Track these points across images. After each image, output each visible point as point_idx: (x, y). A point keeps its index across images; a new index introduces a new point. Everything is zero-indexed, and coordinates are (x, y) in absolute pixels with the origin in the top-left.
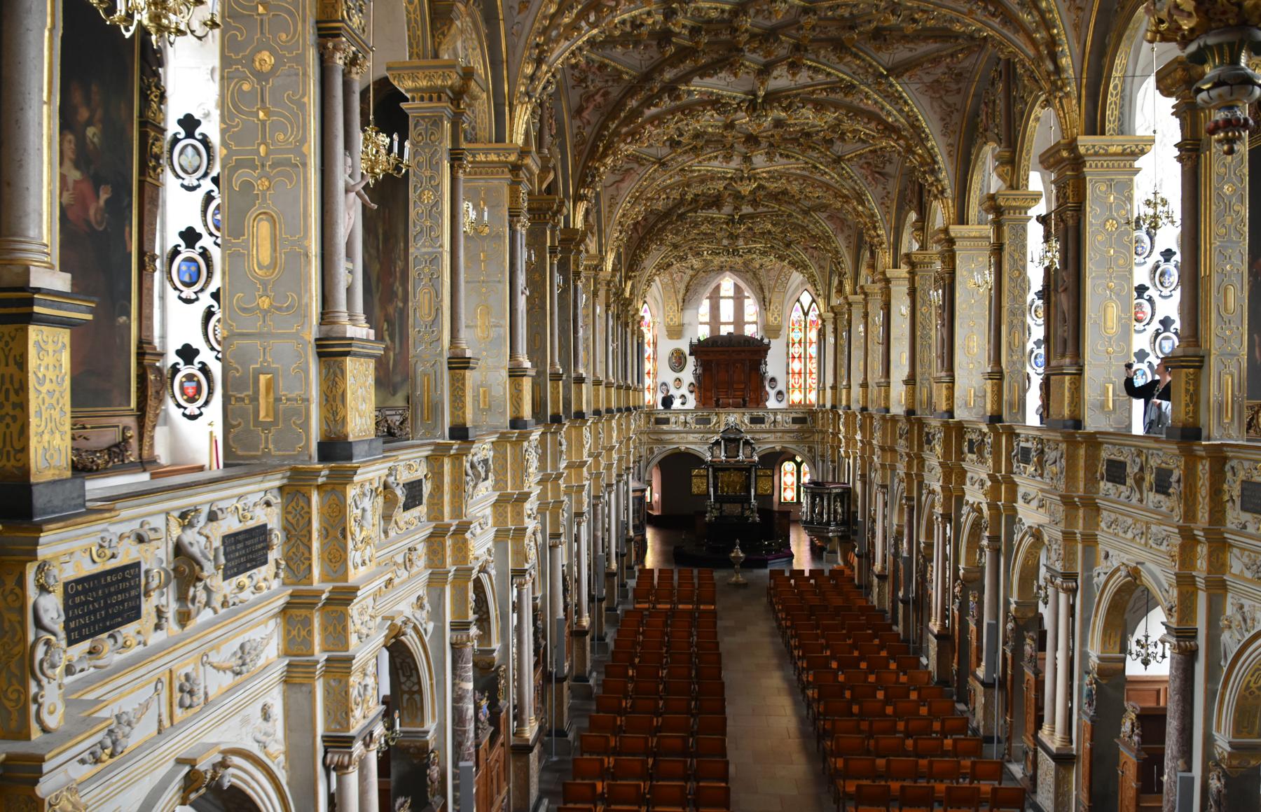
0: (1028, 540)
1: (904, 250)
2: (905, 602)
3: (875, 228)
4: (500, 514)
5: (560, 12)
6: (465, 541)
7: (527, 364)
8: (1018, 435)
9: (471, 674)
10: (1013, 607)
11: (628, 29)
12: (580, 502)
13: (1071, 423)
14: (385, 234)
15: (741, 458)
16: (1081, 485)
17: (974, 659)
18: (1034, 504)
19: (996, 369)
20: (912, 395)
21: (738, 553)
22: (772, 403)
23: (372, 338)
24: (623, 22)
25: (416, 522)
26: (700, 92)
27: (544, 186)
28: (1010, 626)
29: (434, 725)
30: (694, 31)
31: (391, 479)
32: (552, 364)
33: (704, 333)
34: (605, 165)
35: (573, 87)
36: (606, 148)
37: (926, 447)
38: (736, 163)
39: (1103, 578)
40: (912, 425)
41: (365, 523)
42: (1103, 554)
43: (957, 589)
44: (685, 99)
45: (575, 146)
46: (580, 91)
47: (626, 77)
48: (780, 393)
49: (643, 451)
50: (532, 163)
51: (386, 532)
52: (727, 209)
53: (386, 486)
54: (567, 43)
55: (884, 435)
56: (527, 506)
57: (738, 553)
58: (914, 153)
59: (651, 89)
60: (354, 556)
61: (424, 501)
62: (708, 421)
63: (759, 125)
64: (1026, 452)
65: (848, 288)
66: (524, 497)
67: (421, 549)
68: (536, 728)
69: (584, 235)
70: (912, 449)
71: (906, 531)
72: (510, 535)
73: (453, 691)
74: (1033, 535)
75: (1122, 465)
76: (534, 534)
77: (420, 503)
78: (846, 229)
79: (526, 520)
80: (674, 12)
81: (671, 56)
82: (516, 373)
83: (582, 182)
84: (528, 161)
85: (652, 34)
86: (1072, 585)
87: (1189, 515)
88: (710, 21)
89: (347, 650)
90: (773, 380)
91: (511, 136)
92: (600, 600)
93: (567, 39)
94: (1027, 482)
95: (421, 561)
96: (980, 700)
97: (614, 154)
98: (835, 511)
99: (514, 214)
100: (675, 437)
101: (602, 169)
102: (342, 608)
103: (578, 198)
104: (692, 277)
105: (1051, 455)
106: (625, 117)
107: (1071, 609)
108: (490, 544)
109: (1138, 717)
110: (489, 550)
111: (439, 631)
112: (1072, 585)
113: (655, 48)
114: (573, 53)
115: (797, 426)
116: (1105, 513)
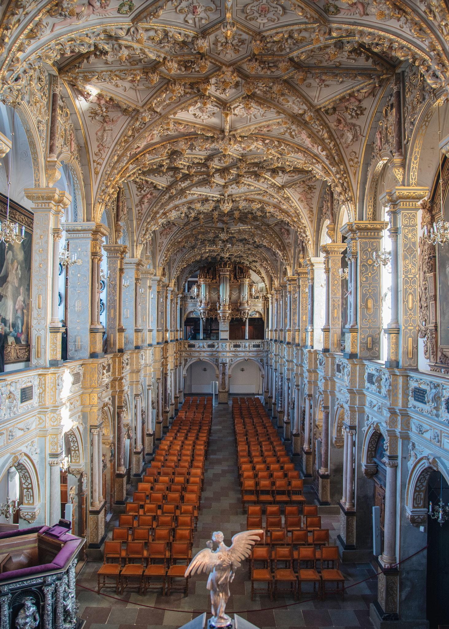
19: (327, 327)
62: (213, 346)
87: (395, 402)
112: (354, 431)
115: (255, 349)
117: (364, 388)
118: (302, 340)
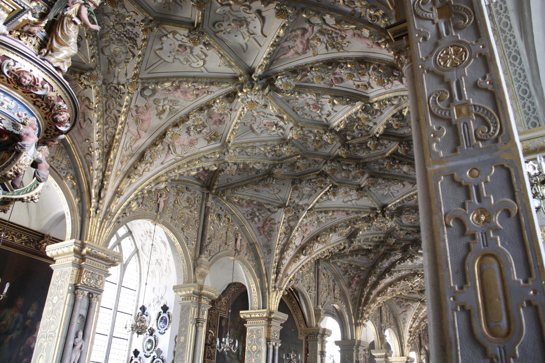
35: (344, 275)
45: (352, 300)
46: (347, 276)
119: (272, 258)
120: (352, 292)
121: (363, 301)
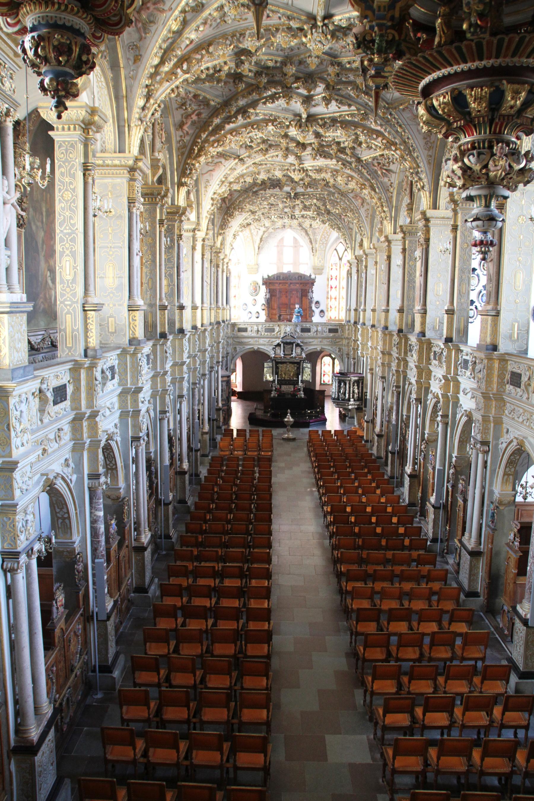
0: (464, 419)
1: (401, 222)
2: (393, 453)
3: (382, 206)
4: (123, 401)
5: (162, 62)
6: (96, 423)
7: (140, 302)
8: (462, 351)
9: (102, 506)
10: (454, 459)
11: (211, 71)
12: (181, 389)
13: (491, 347)
14: (47, 211)
15: (294, 355)
16: (495, 386)
17: (430, 491)
18: (469, 395)
19: (450, 308)
20: (401, 319)
21: (289, 418)
22: (316, 319)
23: (25, 300)
24: (208, 69)
25: (63, 412)
26: (264, 115)
27: (155, 179)
28: (452, 471)
29: (80, 538)
30: (258, 74)
31: (44, 386)
32: (161, 299)
33: (272, 271)
34: (199, 162)
35: (177, 109)
36: (200, 150)
37: (409, 353)
38: (291, 159)
39: (504, 445)
40: (401, 339)
41: (22, 420)
42: (505, 430)
43: (423, 446)
44: (253, 118)
45: (178, 149)
47: (212, 103)
48: (322, 311)
49: (230, 350)
50: (145, 165)
51: (41, 420)
52: (287, 189)
53: (40, 391)
54: (168, 84)
55: (384, 344)
56: (141, 395)
57: (289, 418)
58: (406, 160)
59: (230, 112)
60: (15, 441)
61: (68, 397)
62: (273, 330)
63: (304, 137)
64: (466, 362)
65: (366, 244)
66: (139, 390)
67: (67, 428)
68: (149, 536)
69: (185, 209)
70: (400, 355)
71: (395, 408)
72: (130, 414)
73: (91, 517)
74: (467, 416)
75: (520, 375)
76: (148, 411)
77: (66, 399)
78: (365, 204)
79: (140, 405)
80: (242, 62)
81: (242, 91)
82: (132, 308)
83: (183, 173)
84: (140, 164)
85: (229, 75)
86: (486, 448)
88: (268, 68)
89: (13, 500)
90: (317, 302)
91: (130, 148)
92: (197, 451)
93: (167, 81)
94: (466, 382)
95: (67, 436)
96: (431, 516)
97: (206, 154)
98: (353, 392)
99: (131, 202)
100: (252, 341)
101: (197, 165)
102: (8, 474)
103: (181, 184)
104: (264, 232)
105: (478, 367)
106: (213, 130)
107: (486, 462)
108: (117, 421)
109: (519, 531)
110: (116, 425)
111: (80, 480)
112: (486, 448)
113: (232, 84)
114: (173, 90)
115: (331, 335)
116: (508, 405)
117: (504, 391)
118: (407, 324)
119: (140, 70)
120: (181, 136)
121: (196, 151)
